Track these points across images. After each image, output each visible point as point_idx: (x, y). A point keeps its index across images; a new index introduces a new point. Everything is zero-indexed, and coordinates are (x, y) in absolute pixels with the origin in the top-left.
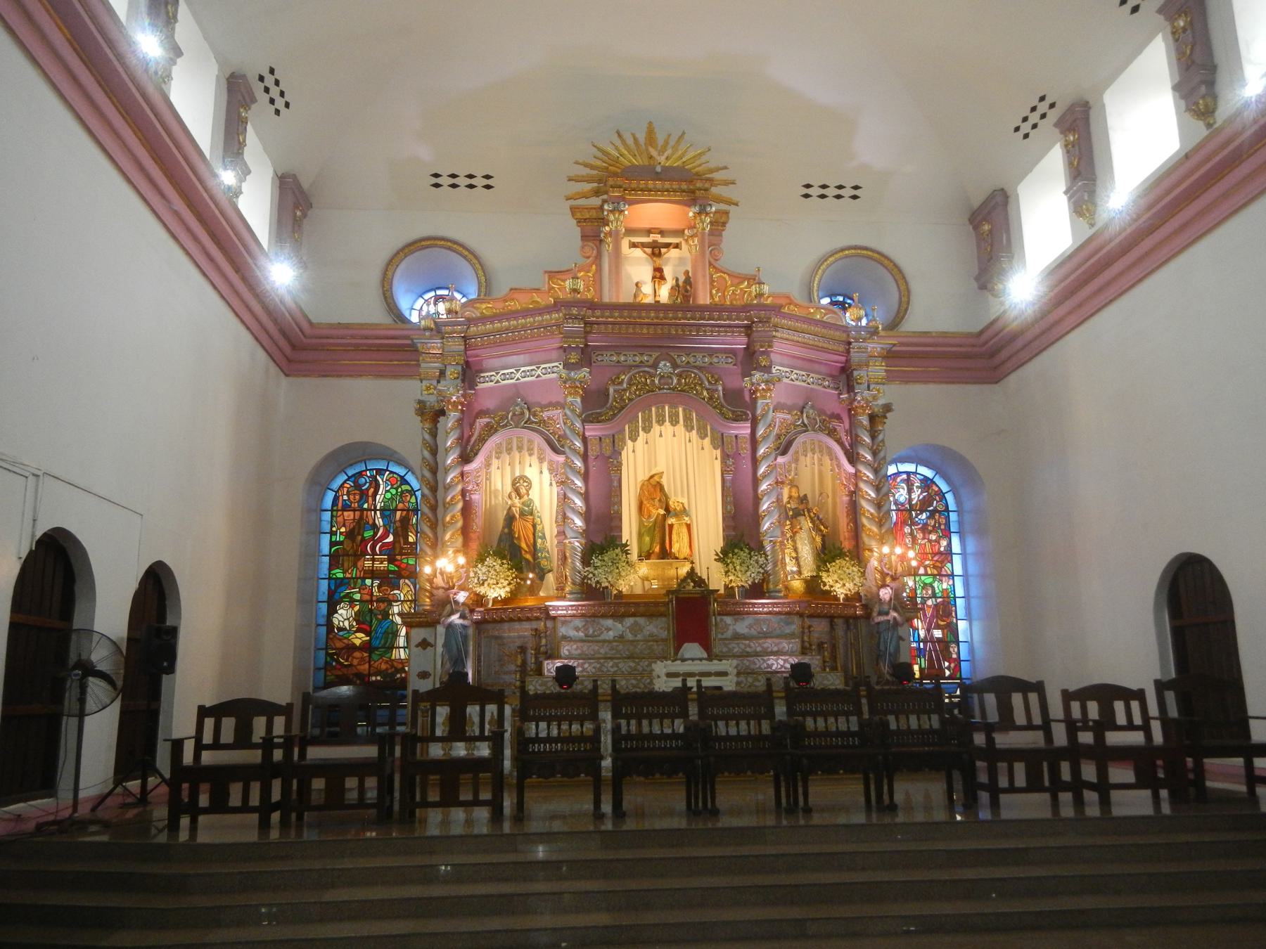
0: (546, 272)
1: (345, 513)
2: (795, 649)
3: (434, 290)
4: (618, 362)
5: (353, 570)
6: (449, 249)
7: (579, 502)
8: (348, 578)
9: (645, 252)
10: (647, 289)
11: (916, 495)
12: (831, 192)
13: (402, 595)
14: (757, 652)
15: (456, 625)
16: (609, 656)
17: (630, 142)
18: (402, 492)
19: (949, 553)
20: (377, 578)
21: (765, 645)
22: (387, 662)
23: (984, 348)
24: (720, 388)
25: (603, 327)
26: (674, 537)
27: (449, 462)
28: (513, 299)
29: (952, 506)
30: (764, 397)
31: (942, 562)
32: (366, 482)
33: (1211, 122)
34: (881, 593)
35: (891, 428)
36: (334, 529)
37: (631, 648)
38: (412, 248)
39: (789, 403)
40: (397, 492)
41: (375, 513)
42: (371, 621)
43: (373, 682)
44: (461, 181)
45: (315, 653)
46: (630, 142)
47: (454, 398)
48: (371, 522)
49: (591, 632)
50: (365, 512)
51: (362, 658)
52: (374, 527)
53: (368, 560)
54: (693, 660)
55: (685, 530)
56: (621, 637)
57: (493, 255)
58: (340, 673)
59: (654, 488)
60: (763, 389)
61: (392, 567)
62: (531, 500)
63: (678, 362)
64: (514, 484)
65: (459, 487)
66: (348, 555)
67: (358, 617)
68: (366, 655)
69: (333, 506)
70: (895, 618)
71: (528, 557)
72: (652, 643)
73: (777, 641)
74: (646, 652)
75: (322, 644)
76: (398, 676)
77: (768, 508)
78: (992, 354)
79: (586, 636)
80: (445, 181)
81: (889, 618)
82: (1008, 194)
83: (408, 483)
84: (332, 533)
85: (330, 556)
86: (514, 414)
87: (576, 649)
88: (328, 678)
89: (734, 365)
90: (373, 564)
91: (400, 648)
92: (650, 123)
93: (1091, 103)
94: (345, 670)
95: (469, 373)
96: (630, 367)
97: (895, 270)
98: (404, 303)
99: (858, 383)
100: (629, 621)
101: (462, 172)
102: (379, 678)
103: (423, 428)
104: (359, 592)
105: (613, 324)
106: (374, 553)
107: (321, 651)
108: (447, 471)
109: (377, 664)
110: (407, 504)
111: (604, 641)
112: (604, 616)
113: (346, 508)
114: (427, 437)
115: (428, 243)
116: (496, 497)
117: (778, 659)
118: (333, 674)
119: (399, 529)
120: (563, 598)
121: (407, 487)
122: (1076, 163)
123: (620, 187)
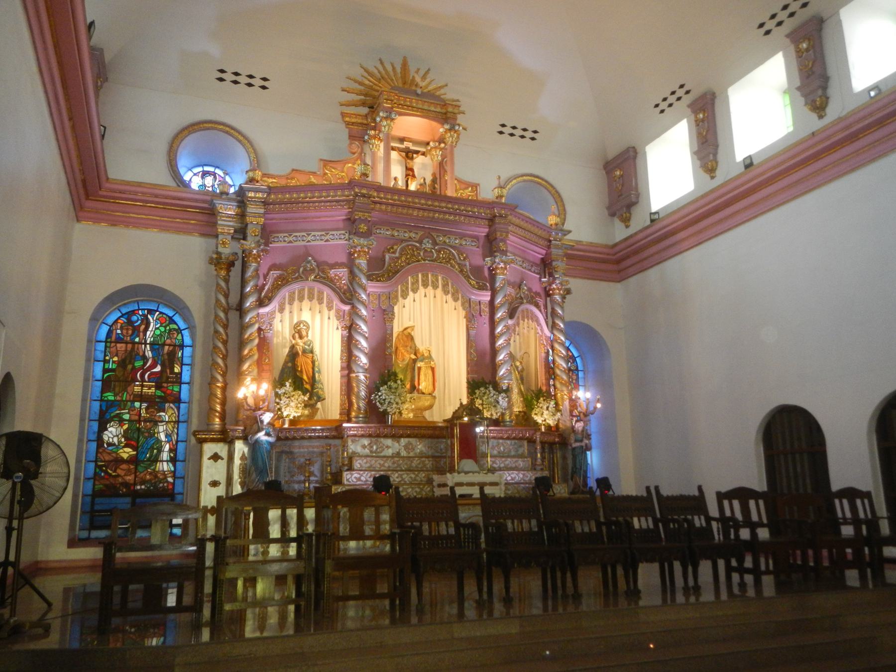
0: (321, 160)
1: (119, 345)
2: (527, 466)
3: (203, 166)
4: (393, 236)
5: (123, 394)
6: (227, 133)
7: (364, 343)
8: (118, 401)
9: (400, 155)
12: (518, 132)
13: (167, 417)
14: (501, 468)
15: (262, 441)
16: (391, 469)
17: (389, 68)
18: (170, 330)
20: (145, 402)
21: (507, 462)
22: (150, 474)
23: (614, 257)
24: (468, 264)
25: (384, 207)
26: (422, 377)
27: (248, 304)
28: (292, 178)
30: (503, 274)
32: (138, 320)
33: (823, 114)
34: (576, 426)
36: (107, 358)
37: (409, 463)
38: (196, 127)
39: (512, 280)
40: (165, 330)
41: (145, 347)
42: (139, 438)
43: (138, 490)
44: (243, 79)
45: (85, 463)
46: (389, 68)
47: (255, 252)
48: (141, 354)
49: (375, 447)
50: (136, 345)
51: (129, 470)
52: (145, 358)
53: (137, 386)
54: (473, 472)
55: (430, 372)
56: (398, 454)
57: (266, 144)
58: (108, 482)
60: (502, 267)
61: (159, 393)
62: (311, 342)
63: (438, 241)
64: (295, 328)
65: (256, 326)
66: (119, 381)
67: (126, 435)
68: (132, 467)
69: (107, 338)
70: (586, 445)
71: (308, 387)
72: (424, 459)
73: (514, 460)
74: (420, 466)
75: (92, 457)
76: (161, 485)
77: (504, 357)
78: (618, 262)
79: (371, 452)
80: (229, 77)
81: (583, 444)
82: (638, 151)
83: (175, 323)
84: (105, 362)
85: (103, 380)
86: (305, 270)
87: (366, 463)
88: (96, 487)
89: (478, 247)
90: (142, 389)
91: (163, 461)
92: (405, 58)
93: (717, 94)
94: (112, 480)
95: (267, 234)
96: (402, 241)
97: (556, 195)
99: (556, 271)
100: (403, 441)
101: (244, 72)
102: (143, 487)
103: (217, 276)
104: (128, 413)
105: (392, 205)
106: (143, 380)
107: (91, 463)
109: (142, 474)
110: (174, 341)
111: (384, 457)
112: (386, 436)
113: (119, 340)
114: (223, 284)
115: (210, 125)
116: (278, 337)
117: (519, 473)
118: (101, 484)
119: (167, 363)
120: (349, 421)
121: (175, 326)
122: (704, 133)
123: (392, 101)
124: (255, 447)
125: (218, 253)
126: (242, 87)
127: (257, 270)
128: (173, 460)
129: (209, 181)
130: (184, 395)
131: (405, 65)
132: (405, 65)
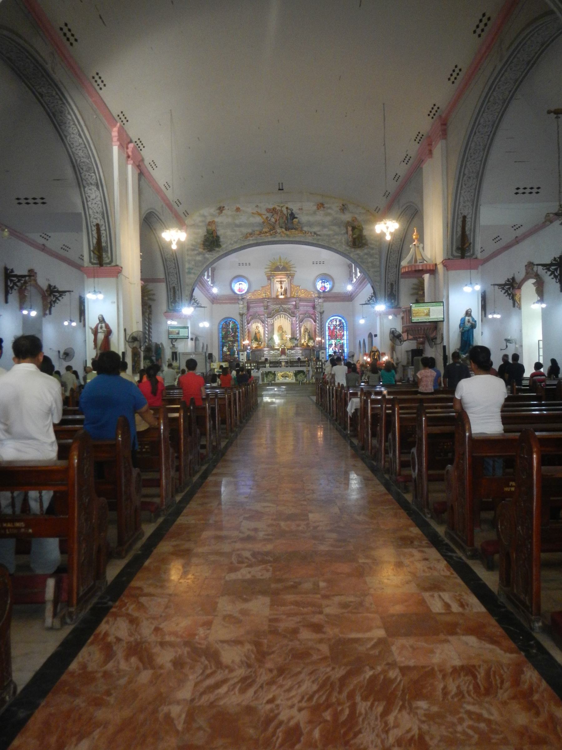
7: (267, 332)
10: (279, 290)
11: (338, 323)
12: (318, 263)
19: (344, 335)
29: (345, 325)
31: (342, 337)
35: (324, 315)
44: (245, 264)
52: (230, 332)
56: (274, 354)
59: (280, 328)
67: (228, 349)
98: (233, 286)
101: (244, 263)
108: (245, 326)
124: (247, 352)
125: (240, 313)
126: (244, 266)
127: (247, 317)
128: (238, 354)
129: (241, 285)
130: (239, 339)
131: (280, 258)
132: (280, 258)
